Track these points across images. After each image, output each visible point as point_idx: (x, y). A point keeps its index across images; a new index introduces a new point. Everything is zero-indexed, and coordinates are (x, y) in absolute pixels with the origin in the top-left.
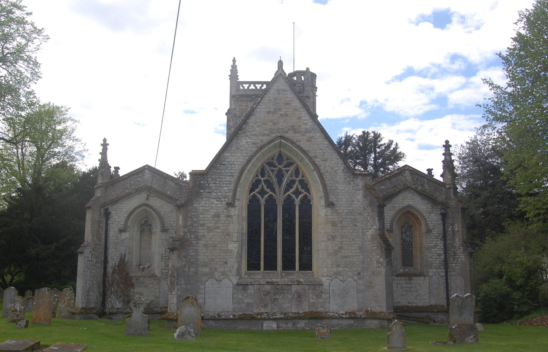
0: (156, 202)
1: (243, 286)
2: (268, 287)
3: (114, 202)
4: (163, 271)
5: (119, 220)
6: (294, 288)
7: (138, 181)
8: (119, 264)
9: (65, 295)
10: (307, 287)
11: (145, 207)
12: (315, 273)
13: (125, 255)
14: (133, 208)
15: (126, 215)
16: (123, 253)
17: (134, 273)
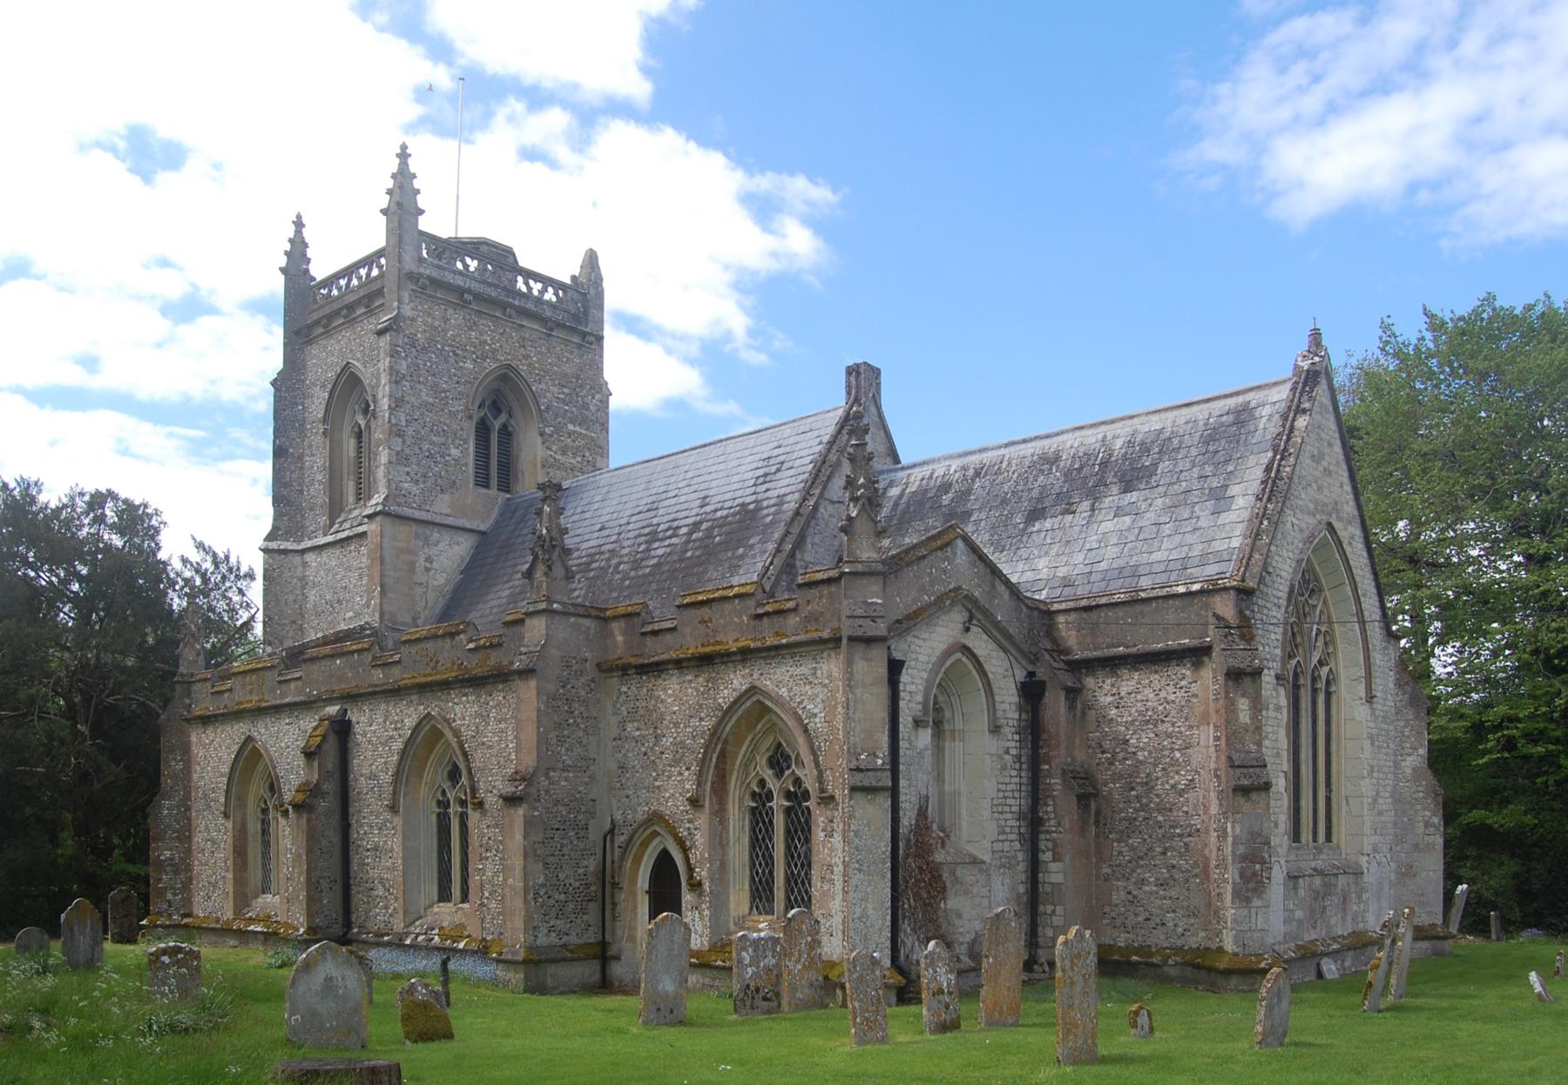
0: (980, 643)
1: (1293, 878)
2: (1318, 881)
3: (907, 623)
4: (998, 846)
5: (913, 688)
6: (1342, 880)
7: (944, 571)
8: (917, 825)
9: (800, 931)
10: (1351, 879)
11: (958, 655)
12: (1343, 847)
13: (927, 797)
14: (937, 653)
15: (925, 675)
16: (924, 792)
17: (939, 857)
